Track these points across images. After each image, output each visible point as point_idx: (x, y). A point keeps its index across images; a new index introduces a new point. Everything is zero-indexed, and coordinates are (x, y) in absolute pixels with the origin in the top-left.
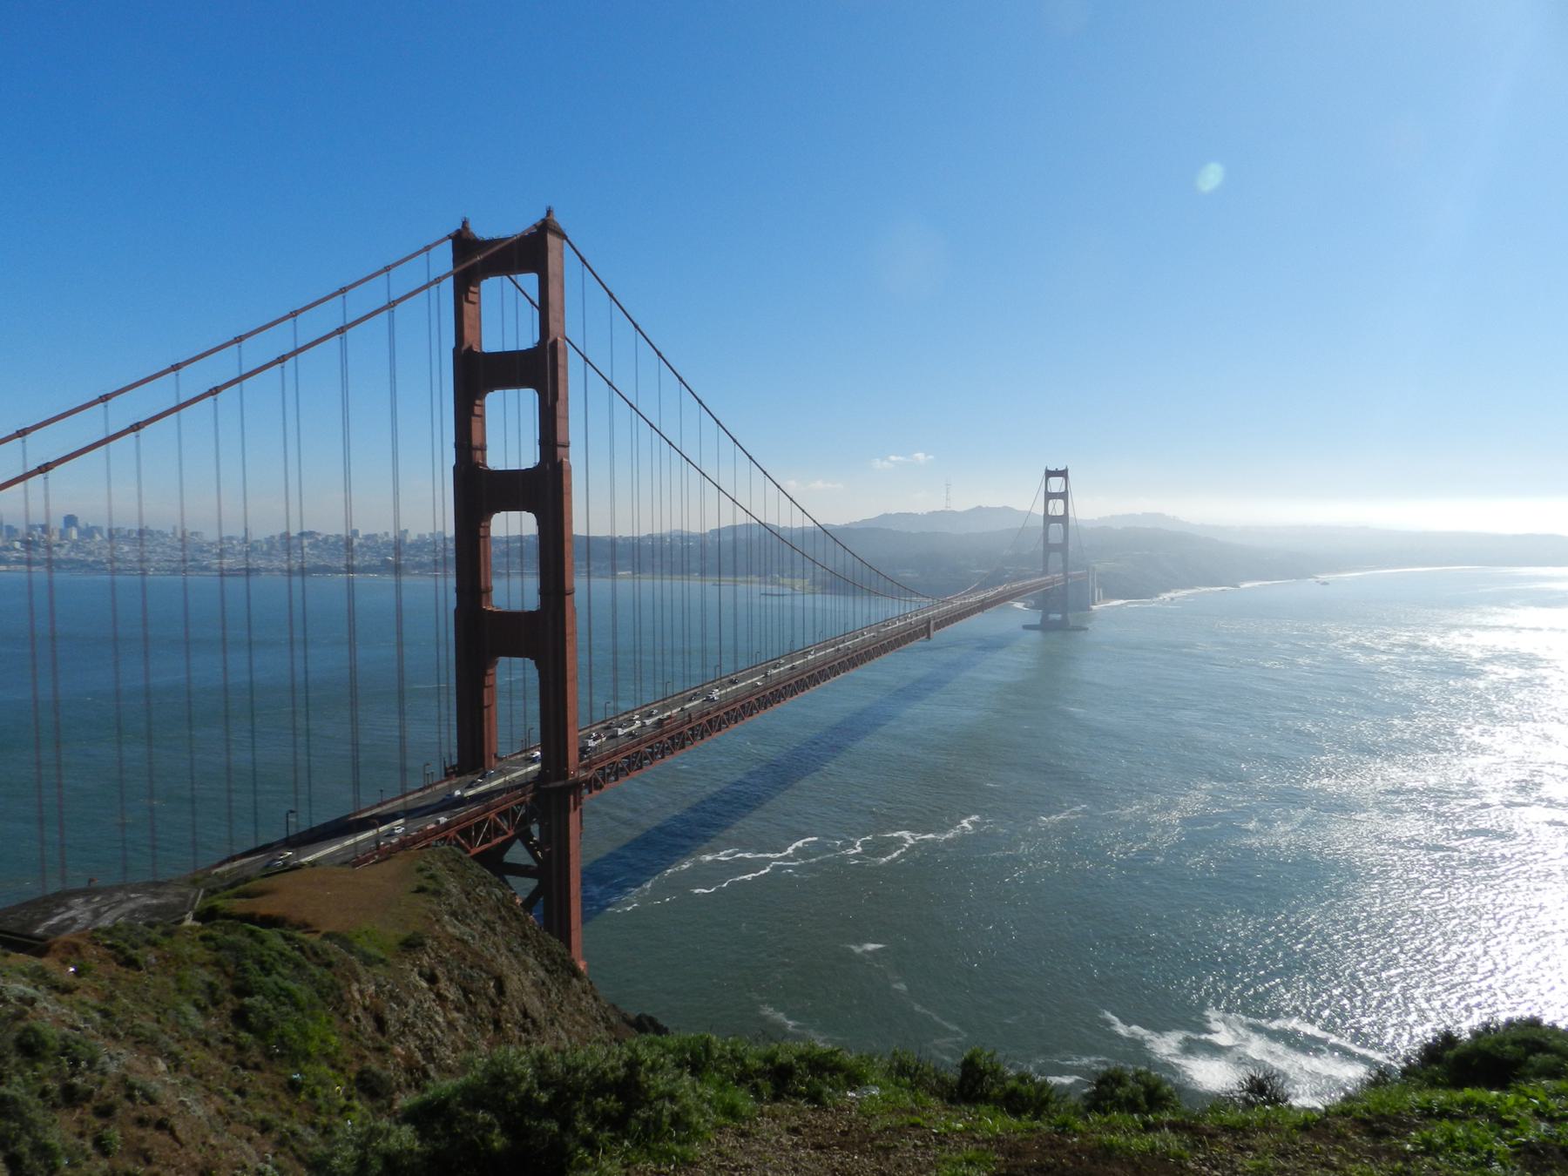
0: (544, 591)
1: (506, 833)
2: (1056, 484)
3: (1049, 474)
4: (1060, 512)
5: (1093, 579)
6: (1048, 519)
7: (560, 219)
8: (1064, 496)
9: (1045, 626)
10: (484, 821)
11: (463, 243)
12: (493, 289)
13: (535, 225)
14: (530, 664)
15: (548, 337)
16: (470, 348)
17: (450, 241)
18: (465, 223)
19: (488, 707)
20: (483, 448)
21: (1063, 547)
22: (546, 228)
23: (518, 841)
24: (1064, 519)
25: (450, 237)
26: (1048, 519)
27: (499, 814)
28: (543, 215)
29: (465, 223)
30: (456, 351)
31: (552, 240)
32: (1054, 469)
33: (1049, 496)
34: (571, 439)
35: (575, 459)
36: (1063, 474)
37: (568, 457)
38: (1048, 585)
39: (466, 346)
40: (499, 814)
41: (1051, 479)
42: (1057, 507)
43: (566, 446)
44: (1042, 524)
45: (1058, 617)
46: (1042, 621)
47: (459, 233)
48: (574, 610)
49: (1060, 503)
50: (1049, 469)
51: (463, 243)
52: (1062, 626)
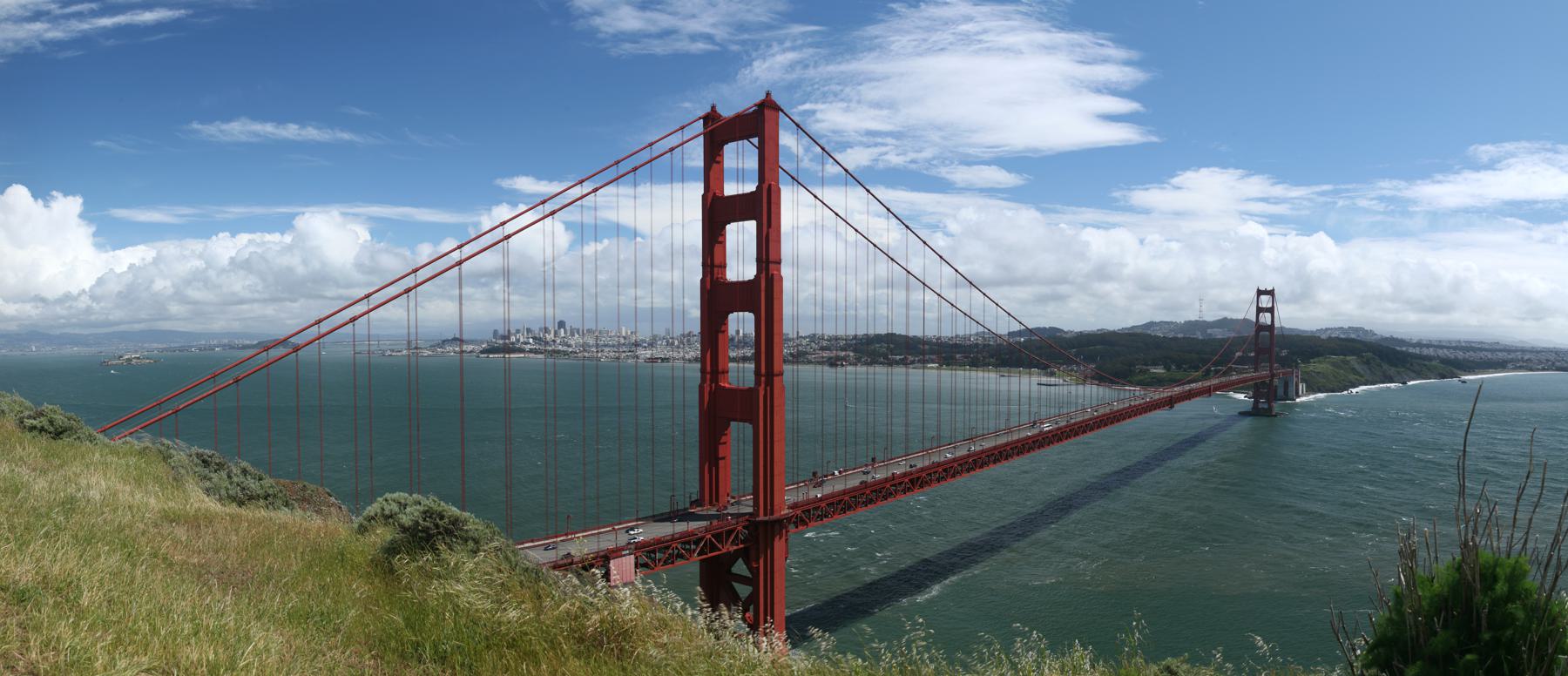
0: (757, 373)
1: (720, 550)
2: (1265, 301)
3: (1260, 293)
4: (1269, 323)
5: (1297, 377)
7: (774, 97)
8: (1271, 310)
11: (711, 118)
13: (755, 105)
14: (748, 428)
16: (715, 194)
17: (702, 120)
18: (713, 108)
19: (723, 458)
20: (723, 266)
23: (740, 559)
25: (700, 118)
26: (1260, 328)
27: (713, 536)
28: (762, 97)
29: (713, 108)
31: (767, 112)
32: (1262, 288)
33: (1260, 310)
36: (1271, 293)
37: (779, 270)
38: (1259, 378)
41: (1263, 297)
42: (1266, 318)
43: (779, 262)
44: (1252, 332)
45: (1266, 406)
46: (1253, 408)
47: (709, 113)
48: (783, 388)
49: (1268, 315)
51: (711, 118)
52: (1268, 413)
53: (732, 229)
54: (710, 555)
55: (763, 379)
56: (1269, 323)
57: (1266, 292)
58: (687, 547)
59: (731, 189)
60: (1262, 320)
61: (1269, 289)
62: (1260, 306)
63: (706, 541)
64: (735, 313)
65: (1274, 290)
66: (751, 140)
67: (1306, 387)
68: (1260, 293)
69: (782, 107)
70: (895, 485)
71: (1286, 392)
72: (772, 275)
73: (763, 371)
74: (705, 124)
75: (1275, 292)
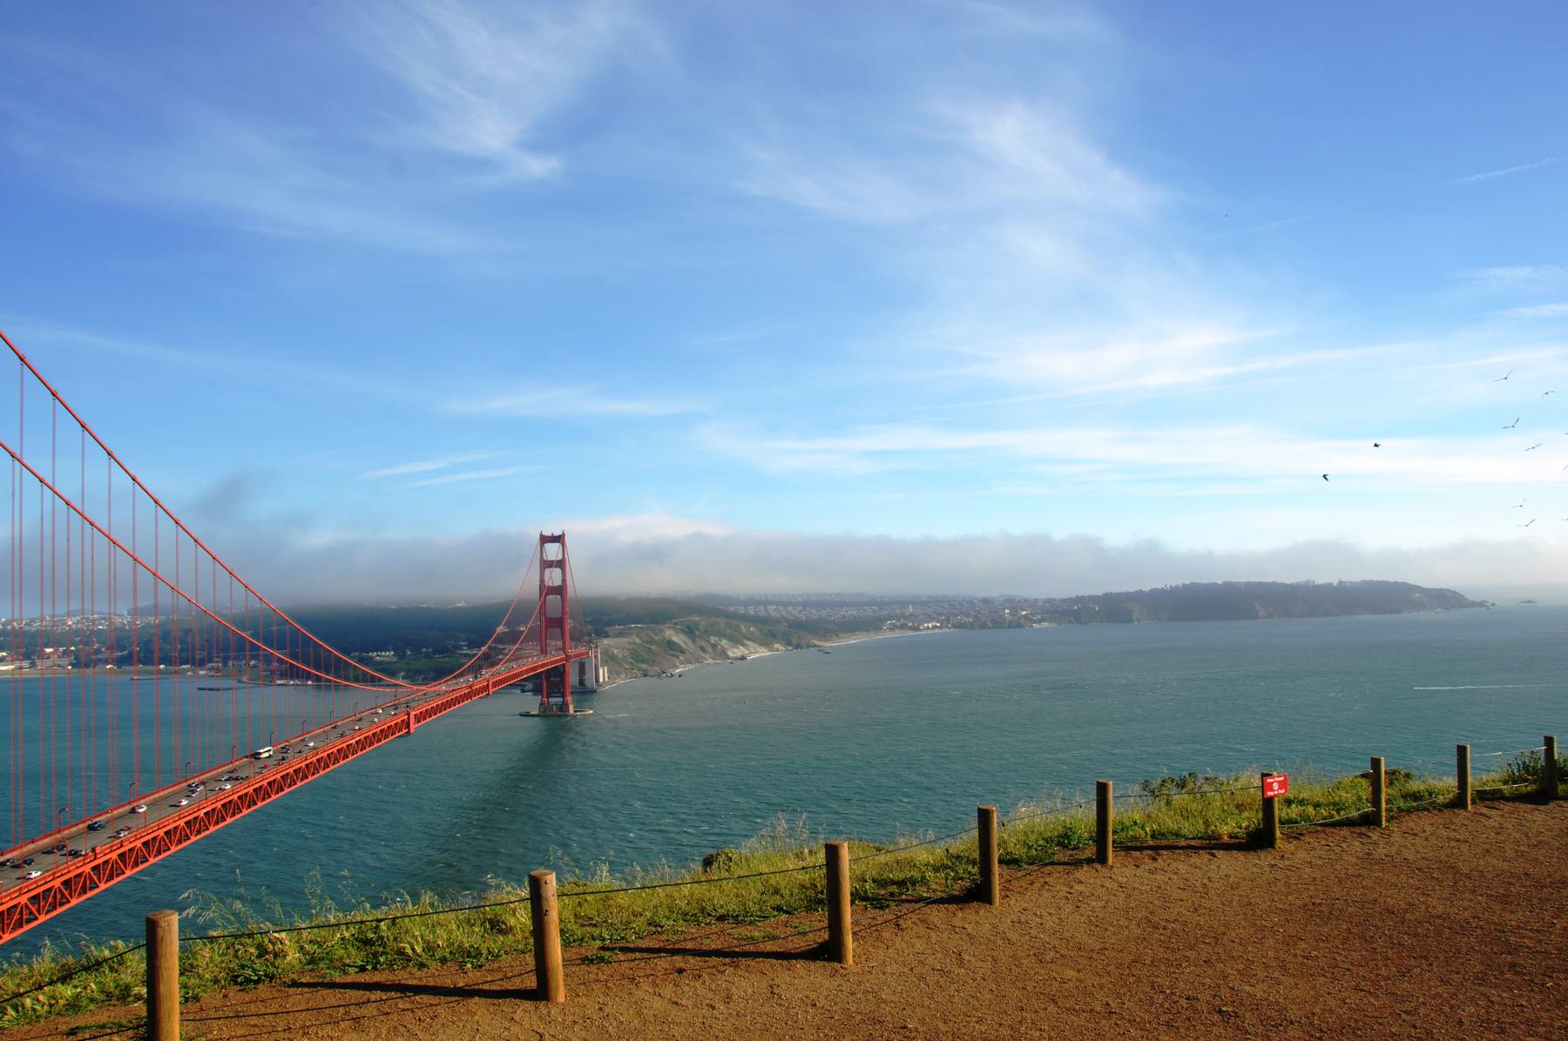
2: (553, 551)
3: (545, 540)
4: (558, 582)
5: (596, 657)
6: (546, 590)
8: (561, 564)
9: (545, 713)
21: (558, 623)
24: (560, 590)
26: (546, 590)
32: (547, 533)
36: (559, 539)
41: (546, 545)
42: (553, 578)
49: (558, 571)
50: (544, 534)
60: (548, 582)
61: (556, 534)
62: (545, 558)
65: (564, 535)
67: (609, 672)
70: (95, 868)
71: (582, 682)
75: (566, 538)
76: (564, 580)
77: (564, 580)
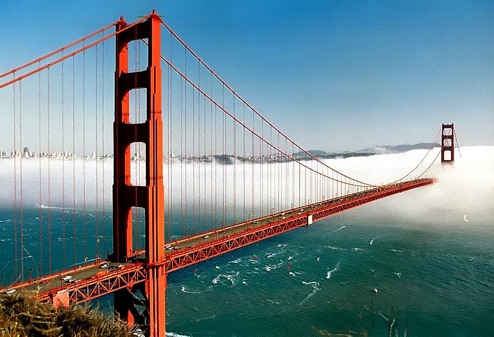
2: (448, 132)
3: (444, 127)
7: (157, 14)
8: (451, 137)
10: (116, 278)
12: (131, 44)
15: (151, 65)
16: (122, 71)
22: (153, 17)
30: (116, 73)
31: (153, 22)
33: (444, 137)
34: (162, 111)
35: (164, 118)
36: (451, 126)
37: (160, 117)
39: (120, 73)
40: (122, 276)
41: (445, 129)
42: (448, 143)
51: (120, 25)
53: (132, 92)
54: (120, 288)
55: (151, 181)
56: (451, 146)
57: (448, 126)
58: (106, 284)
59: (132, 69)
60: (445, 145)
61: (449, 124)
62: (444, 135)
63: (118, 279)
64: (134, 143)
65: (453, 124)
66: (143, 39)
68: (444, 127)
69: (162, 20)
72: (156, 120)
73: (151, 175)
74: (117, 28)
76: (453, 144)
77: (453, 144)
